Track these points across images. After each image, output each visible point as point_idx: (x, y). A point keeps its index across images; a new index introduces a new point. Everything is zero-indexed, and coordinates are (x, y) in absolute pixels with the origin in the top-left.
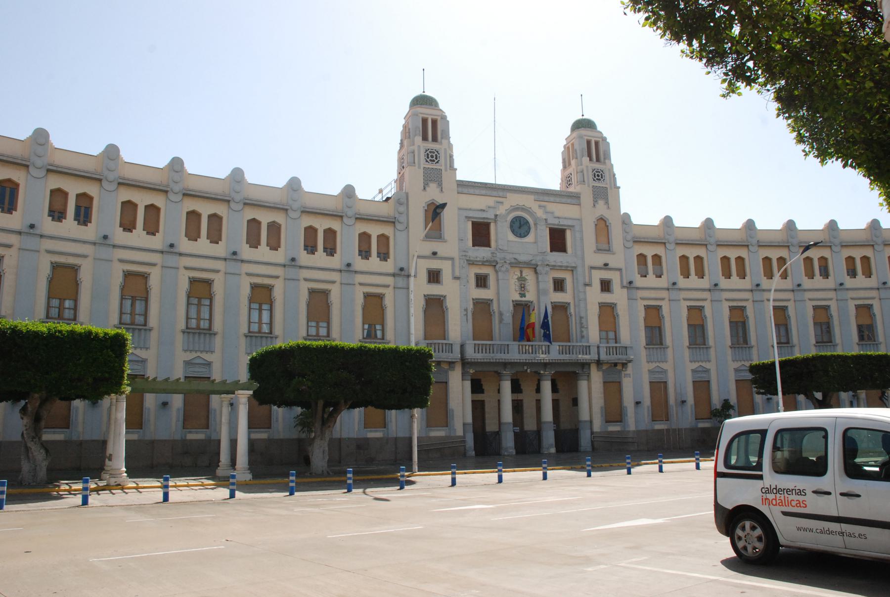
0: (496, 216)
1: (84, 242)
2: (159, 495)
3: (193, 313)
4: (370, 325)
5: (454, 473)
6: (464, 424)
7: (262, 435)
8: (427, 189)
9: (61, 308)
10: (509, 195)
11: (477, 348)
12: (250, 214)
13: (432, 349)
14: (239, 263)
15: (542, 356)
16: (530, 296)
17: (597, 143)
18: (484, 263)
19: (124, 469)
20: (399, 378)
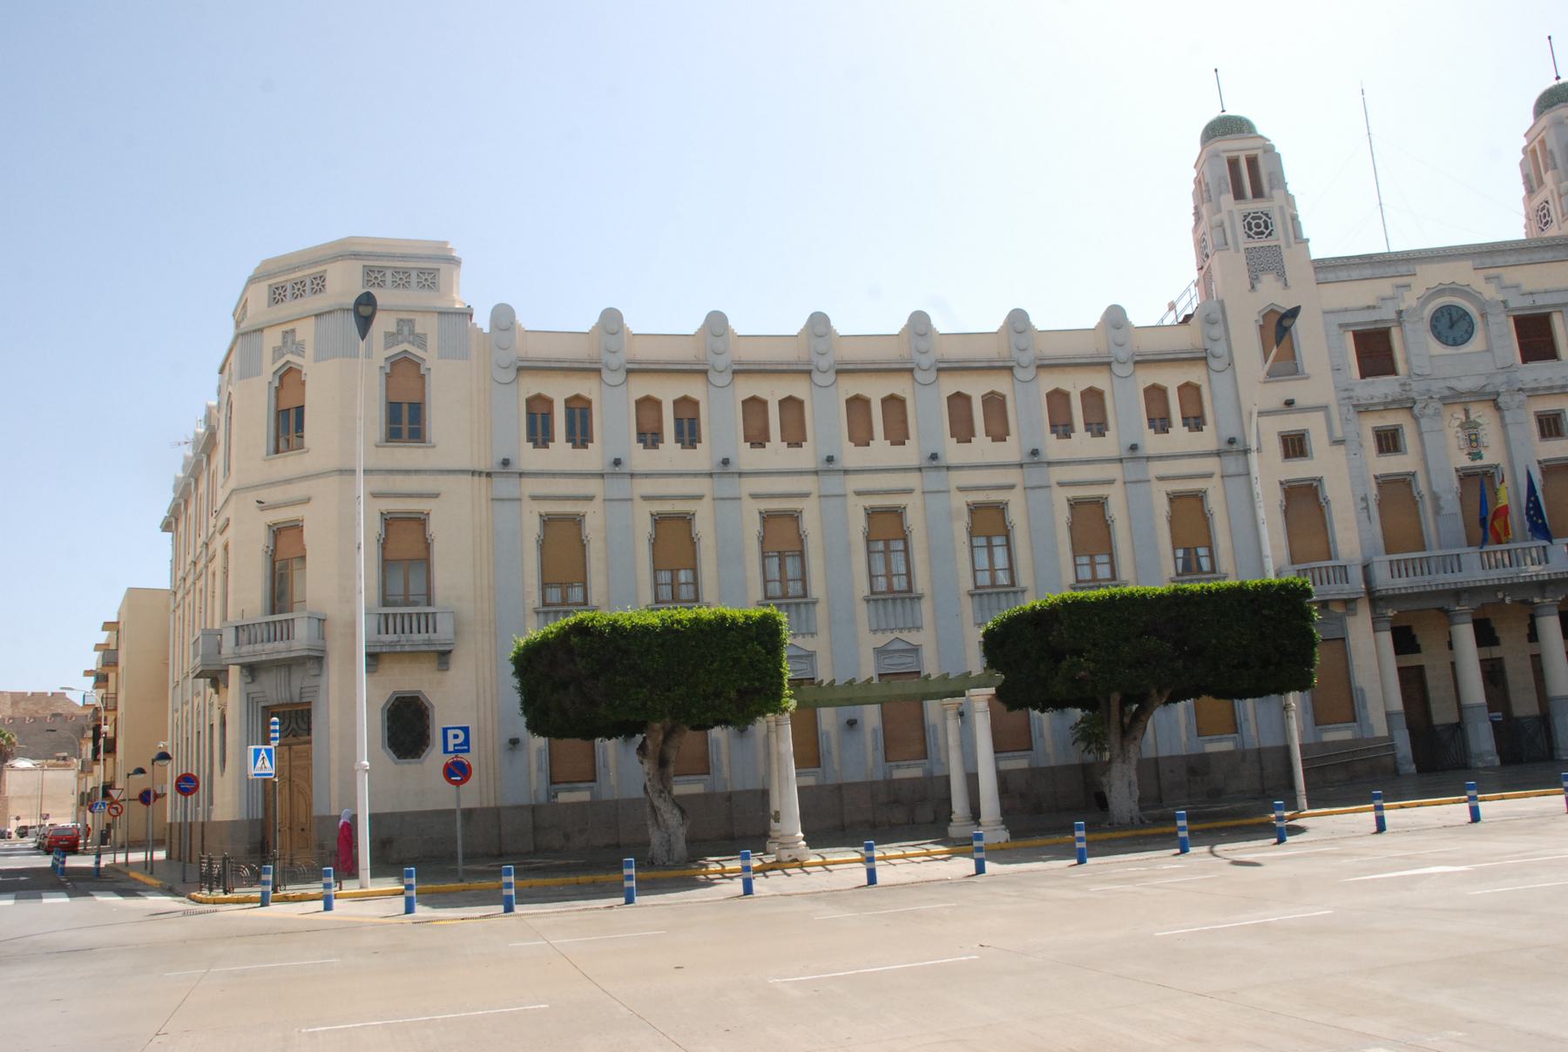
0: (1400, 313)
1: (696, 475)
2: (861, 874)
3: (879, 568)
4: (1187, 550)
5: (1379, 808)
6: (1388, 715)
7: (1018, 763)
8: (1258, 286)
9: (674, 584)
10: (1418, 269)
11: (1396, 568)
12: (950, 385)
13: (1309, 579)
14: (944, 473)
15: (1536, 568)
16: (1491, 456)
18: (1388, 406)
19: (801, 835)
20: (1249, 639)
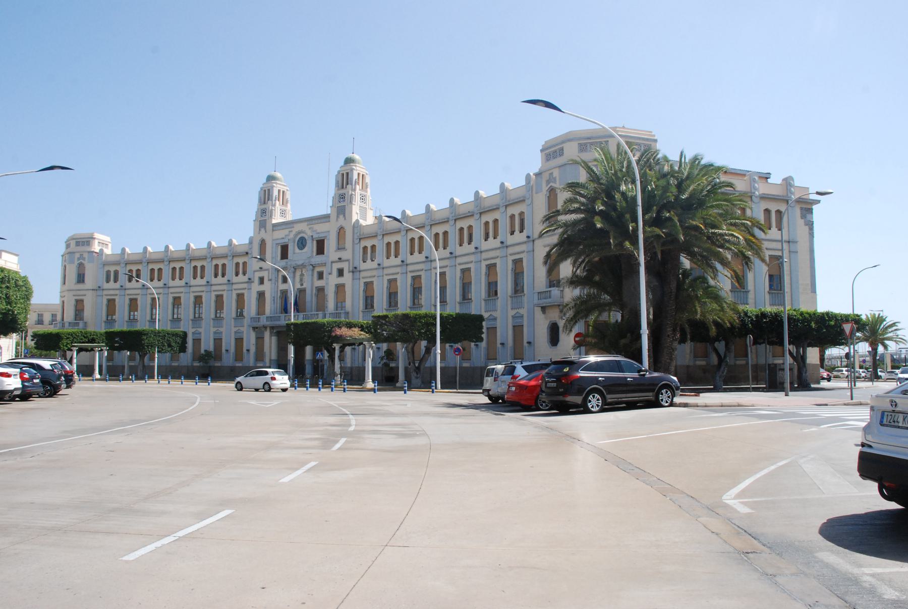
6: (271, 360)
17: (348, 174)
